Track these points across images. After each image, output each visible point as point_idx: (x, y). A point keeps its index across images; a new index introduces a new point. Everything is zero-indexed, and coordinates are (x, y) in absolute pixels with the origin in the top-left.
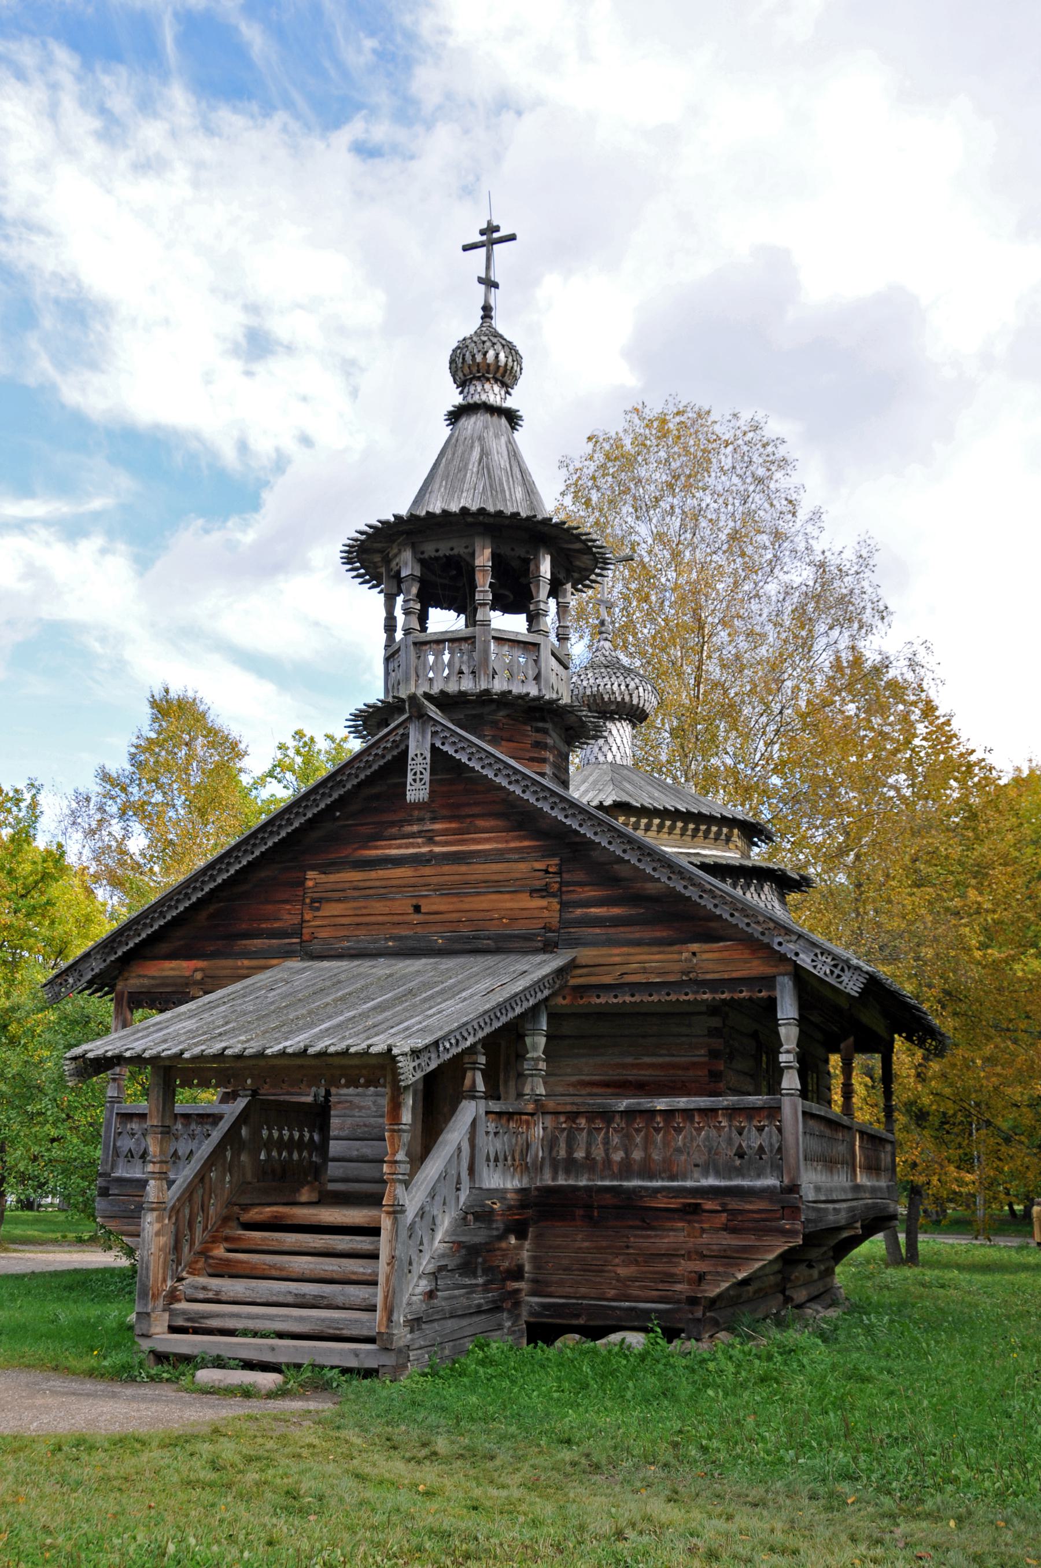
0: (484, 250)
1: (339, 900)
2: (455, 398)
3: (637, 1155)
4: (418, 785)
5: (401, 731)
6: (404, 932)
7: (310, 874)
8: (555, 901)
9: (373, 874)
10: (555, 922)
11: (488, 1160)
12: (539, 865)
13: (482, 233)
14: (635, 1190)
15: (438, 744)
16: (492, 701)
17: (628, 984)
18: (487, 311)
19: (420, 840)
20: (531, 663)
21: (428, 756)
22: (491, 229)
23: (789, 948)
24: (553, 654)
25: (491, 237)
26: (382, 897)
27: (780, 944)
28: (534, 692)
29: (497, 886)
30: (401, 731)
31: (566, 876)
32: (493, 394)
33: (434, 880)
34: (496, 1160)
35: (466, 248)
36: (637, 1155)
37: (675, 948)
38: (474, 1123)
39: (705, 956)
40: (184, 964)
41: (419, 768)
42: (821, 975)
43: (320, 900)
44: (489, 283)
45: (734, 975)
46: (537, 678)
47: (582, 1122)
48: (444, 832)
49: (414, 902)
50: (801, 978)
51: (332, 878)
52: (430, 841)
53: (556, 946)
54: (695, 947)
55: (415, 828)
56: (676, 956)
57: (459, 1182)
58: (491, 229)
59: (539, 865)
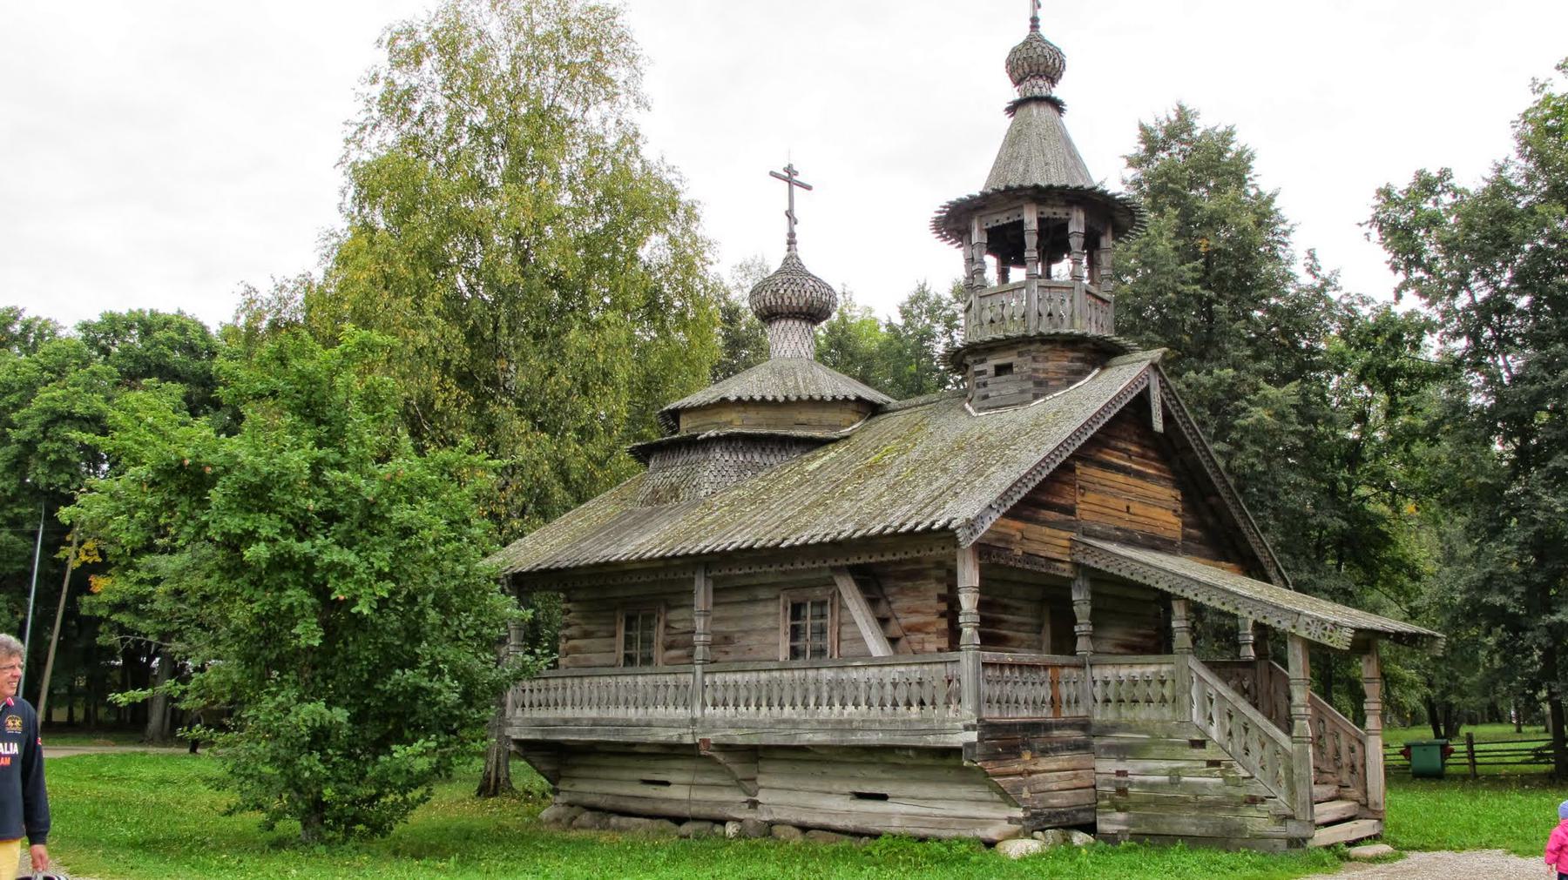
1: (1095, 491)
18: (1035, 22)
52: (1130, 459)
55: (1122, 445)
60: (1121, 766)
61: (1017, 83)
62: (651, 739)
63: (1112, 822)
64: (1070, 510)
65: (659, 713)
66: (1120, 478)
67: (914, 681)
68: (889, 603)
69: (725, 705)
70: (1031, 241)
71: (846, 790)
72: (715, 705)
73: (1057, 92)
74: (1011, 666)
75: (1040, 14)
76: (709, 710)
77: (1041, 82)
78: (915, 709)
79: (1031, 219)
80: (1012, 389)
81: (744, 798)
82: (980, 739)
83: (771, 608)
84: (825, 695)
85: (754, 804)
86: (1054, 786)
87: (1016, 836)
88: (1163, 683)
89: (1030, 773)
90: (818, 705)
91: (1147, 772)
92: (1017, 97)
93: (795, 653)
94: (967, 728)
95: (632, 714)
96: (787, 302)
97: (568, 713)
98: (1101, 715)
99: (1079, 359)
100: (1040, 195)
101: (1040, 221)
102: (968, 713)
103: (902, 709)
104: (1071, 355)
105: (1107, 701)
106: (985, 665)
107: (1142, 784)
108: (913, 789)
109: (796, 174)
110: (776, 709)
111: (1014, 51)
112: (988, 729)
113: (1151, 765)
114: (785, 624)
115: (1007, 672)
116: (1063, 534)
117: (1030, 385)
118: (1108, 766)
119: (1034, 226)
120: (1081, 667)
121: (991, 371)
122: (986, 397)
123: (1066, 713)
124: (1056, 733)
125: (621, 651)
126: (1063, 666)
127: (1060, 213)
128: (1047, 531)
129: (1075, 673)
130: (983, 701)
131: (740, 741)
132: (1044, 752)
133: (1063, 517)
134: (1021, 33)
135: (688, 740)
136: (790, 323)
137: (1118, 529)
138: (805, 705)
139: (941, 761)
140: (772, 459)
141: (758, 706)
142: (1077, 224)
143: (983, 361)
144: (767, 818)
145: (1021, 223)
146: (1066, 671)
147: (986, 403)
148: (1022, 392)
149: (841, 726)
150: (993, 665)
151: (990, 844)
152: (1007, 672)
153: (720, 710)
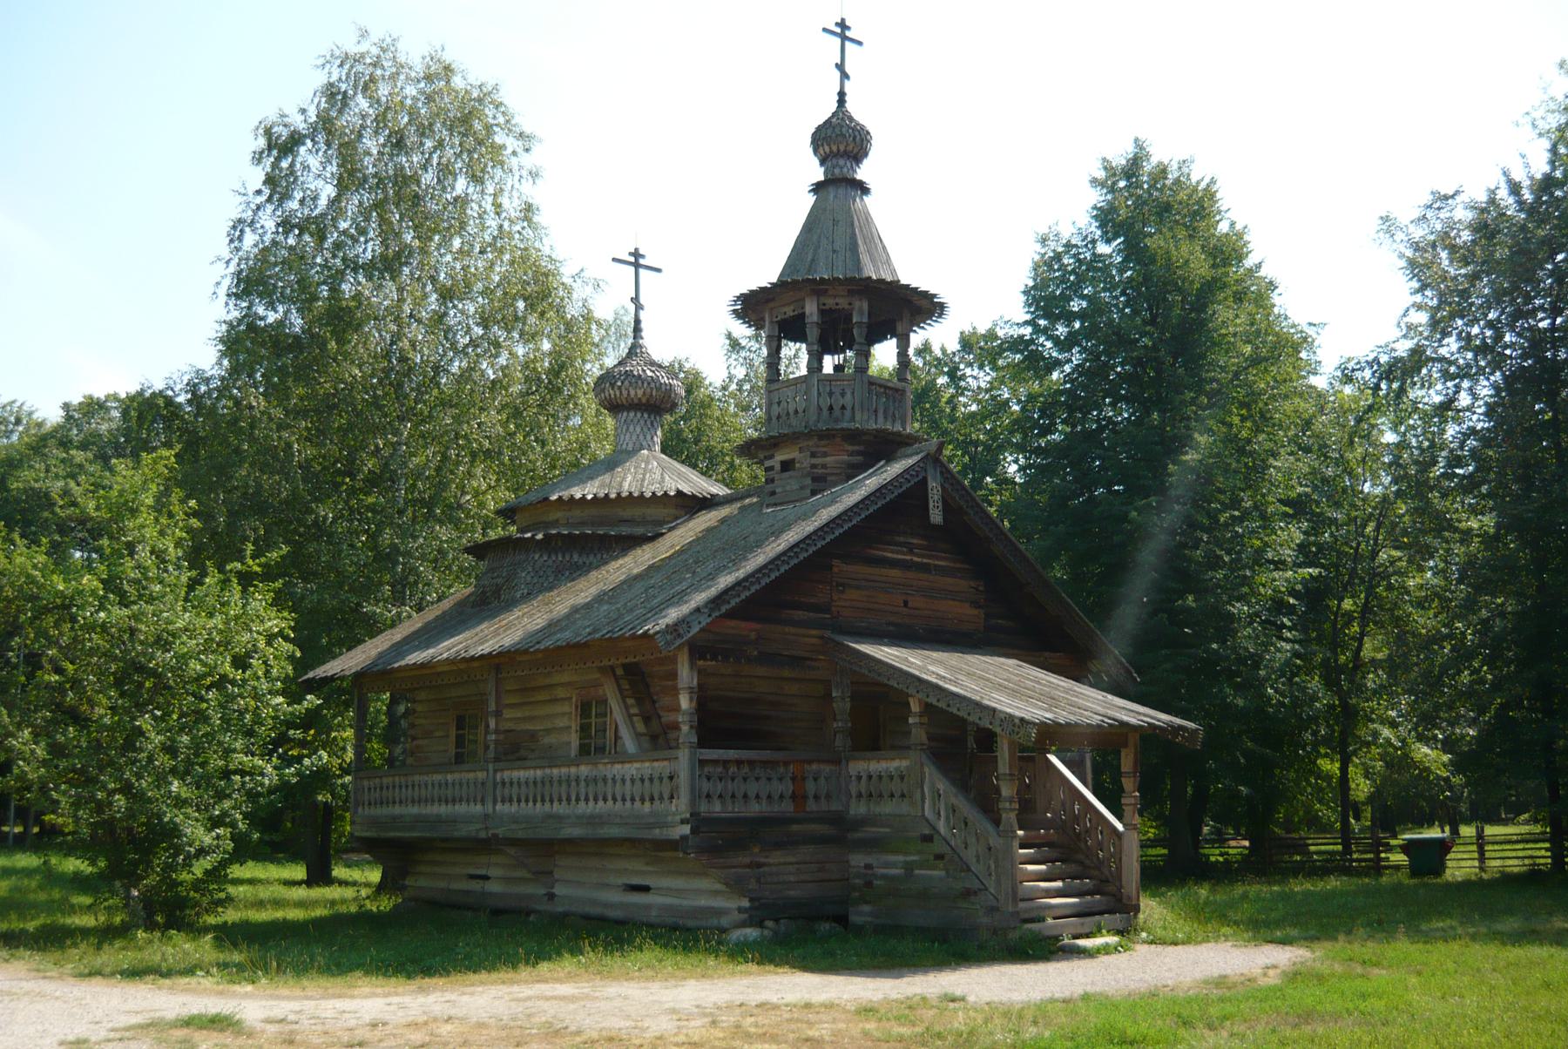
0: (847, 43)
1: (858, 588)
7: (835, 562)
12: (972, 584)
35: (860, 43)
40: (743, 624)
43: (842, 585)
48: (920, 547)
51: (851, 568)
52: (911, 552)
55: (902, 539)
58: (842, 25)
60: (870, 860)
61: (823, 162)
62: (456, 834)
63: (861, 914)
64: (826, 609)
65: (461, 809)
66: (895, 573)
67: (646, 777)
68: (654, 702)
69: (511, 800)
70: (813, 333)
71: (620, 881)
72: (503, 801)
73: (863, 173)
74: (739, 763)
75: (849, 87)
76: (499, 807)
77: (841, 162)
78: (647, 804)
79: (811, 309)
80: (793, 485)
81: (543, 891)
82: (693, 831)
83: (566, 708)
84: (583, 791)
85: (551, 896)
86: (792, 879)
87: (743, 925)
88: (902, 778)
89: (760, 865)
90: (578, 800)
91: (887, 865)
92: (822, 178)
93: (584, 750)
94: (683, 822)
95: (443, 810)
96: (625, 393)
97: (397, 810)
98: (858, 809)
99: (859, 453)
100: (818, 288)
101: (823, 312)
102: (681, 806)
103: (638, 804)
104: (851, 448)
105: (860, 795)
106: (702, 763)
107: (884, 877)
108: (666, 882)
109: (643, 256)
110: (547, 805)
111: (819, 129)
112: (698, 822)
113: (892, 858)
114: (575, 726)
115: (733, 769)
116: (814, 632)
117: (808, 481)
118: (858, 860)
119: (815, 318)
120: (837, 762)
121: (778, 467)
122: (773, 493)
123: (812, 806)
124: (795, 827)
125: (452, 751)
126: (810, 762)
127: (843, 303)
128: (793, 630)
129: (827, 768)
130: (695, 796)
131: (521, 835)
132: (778, 845)
134: (826, 109)
135: (483, 835)
136: (632, 414)
137: (889, 624)
138: (569, 800)
139: (660, 849)
140: (591, 557)
141: (535, 802)
142: (860, 312)
143: (772, 457)
144: (560, 909)
145: (803, 314)
146: (814, 767)
147: (772, 500)
148: (802, 488)
149: (594, 820)
150: (715, 762)
151: (723, 931)
152: (733, 769)
153: (507, 805)
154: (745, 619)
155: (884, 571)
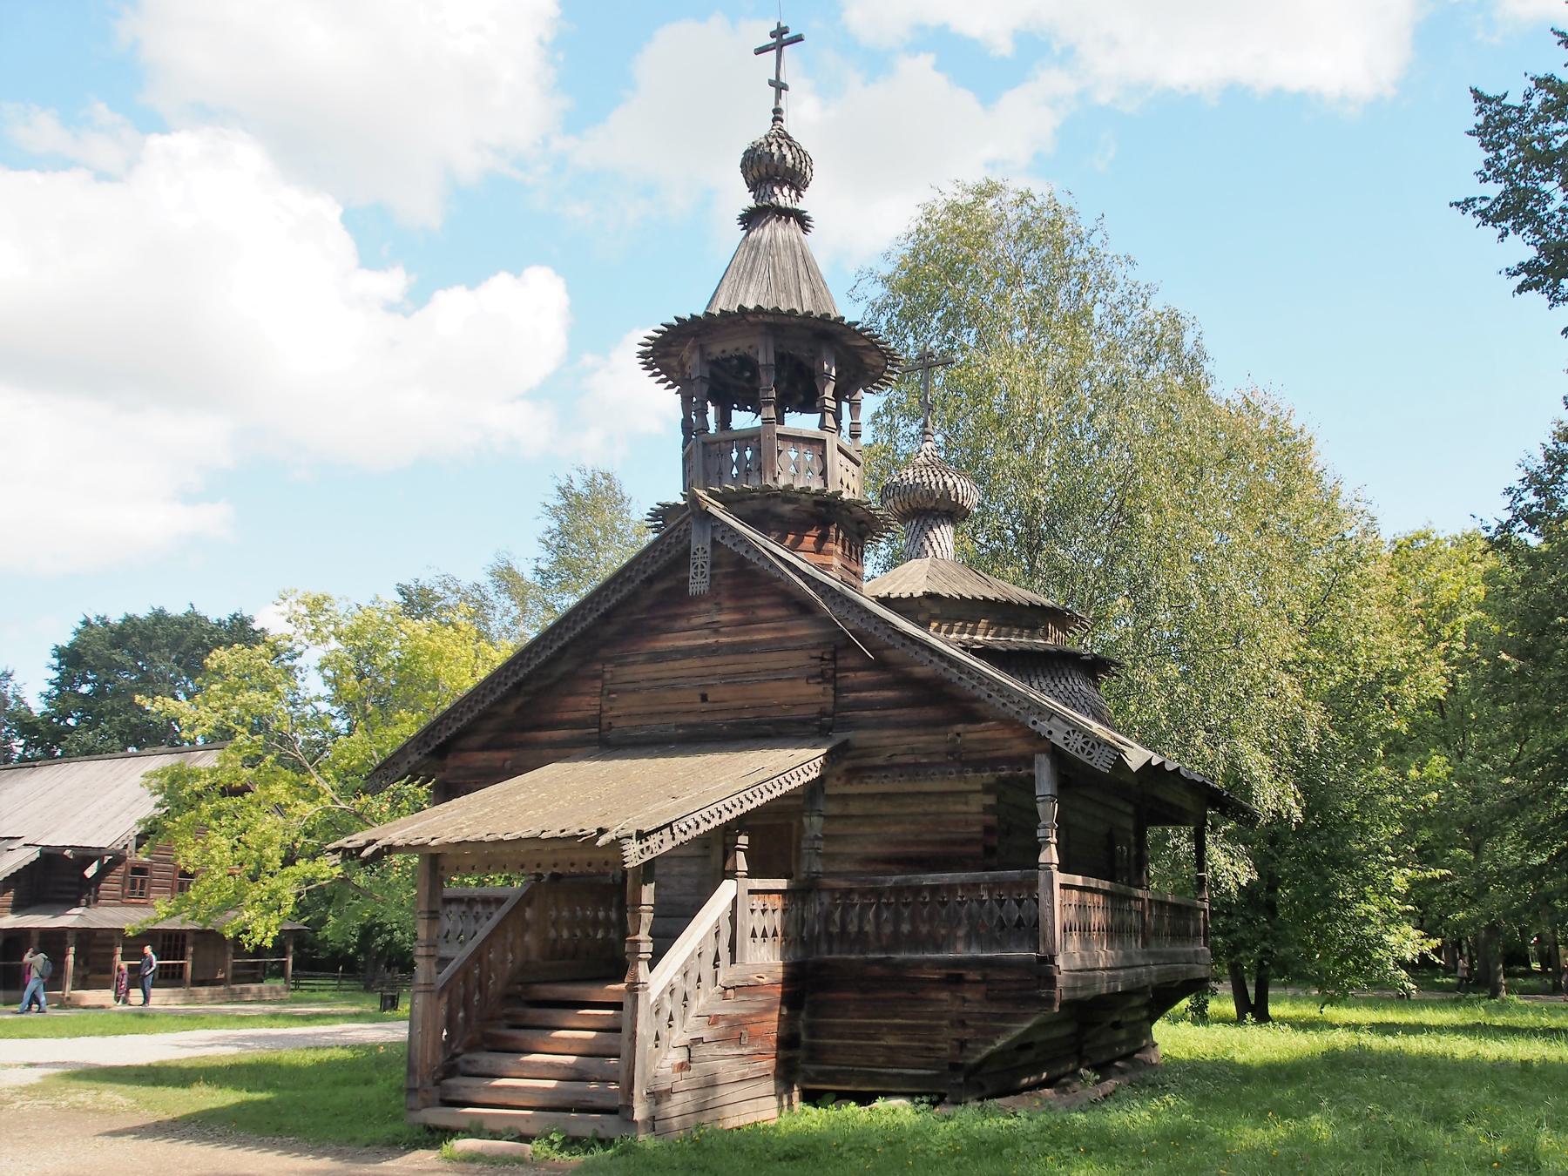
0: (774, 52)
1: (634, 691)
2: (748, 200)
3: (924, 929)
4: (699, 579)
5: (684, 527)
6: (693, 719)
7: (609, 667)
8: (829, 686)
9: (663, 666)
10: (830, 708)
11: (754, 935)
12: (815, 653)
13: (772, 36)
14: (904, 964)
15: (719, 538)
16: (776, 496)
17: (899, 766)
19: (706, 632)
20: (817, 458)
21: (708, 549)
22: (780, 32)
23: (1043, 726)
24: (840, 450)
25: (782, 39)
26: (673, 688)
27: (1034, 723)
28: (816, 485)
29: (776, 675)
30: (684, 527)
31: (841, 663)
32: (784, 197)
33: (720, 670)
34: (764, 935)
36: (906, 928)
37: (942, 729)
38: (735, 901)
39: (969, 736)
41: (699, 562)
42: (1073, 752)
44: (779, 87)
45: (999, 753)
46: (823, 474)
47: (856, 899)
49: (702, 691)
50: (1057, 754)
51: (626, 670)
52: (716, 631)
53: (830, 729)
54: (959, 728)
56: (941, 738)
57: (717, 958)
59: (815, 653)
64: (597, 721)
115: (478, 908)
133: (576, 732)
137: (678, 727)
152: (478, 908)
154: (499, 748)
155: (688, 663)
